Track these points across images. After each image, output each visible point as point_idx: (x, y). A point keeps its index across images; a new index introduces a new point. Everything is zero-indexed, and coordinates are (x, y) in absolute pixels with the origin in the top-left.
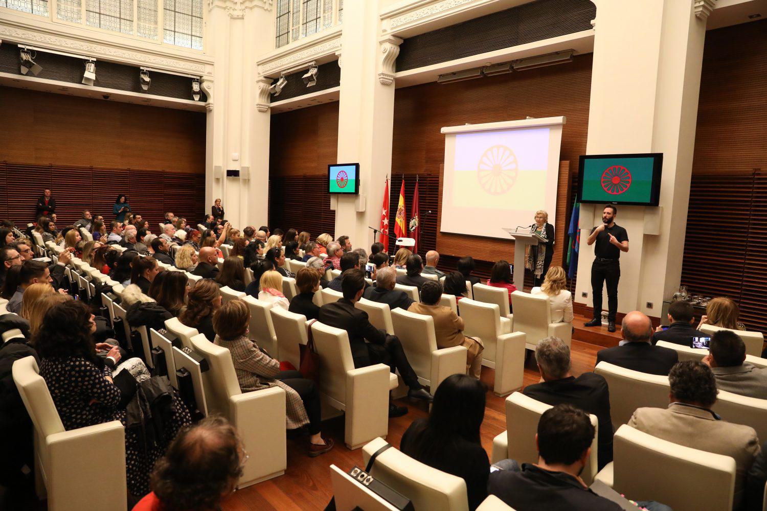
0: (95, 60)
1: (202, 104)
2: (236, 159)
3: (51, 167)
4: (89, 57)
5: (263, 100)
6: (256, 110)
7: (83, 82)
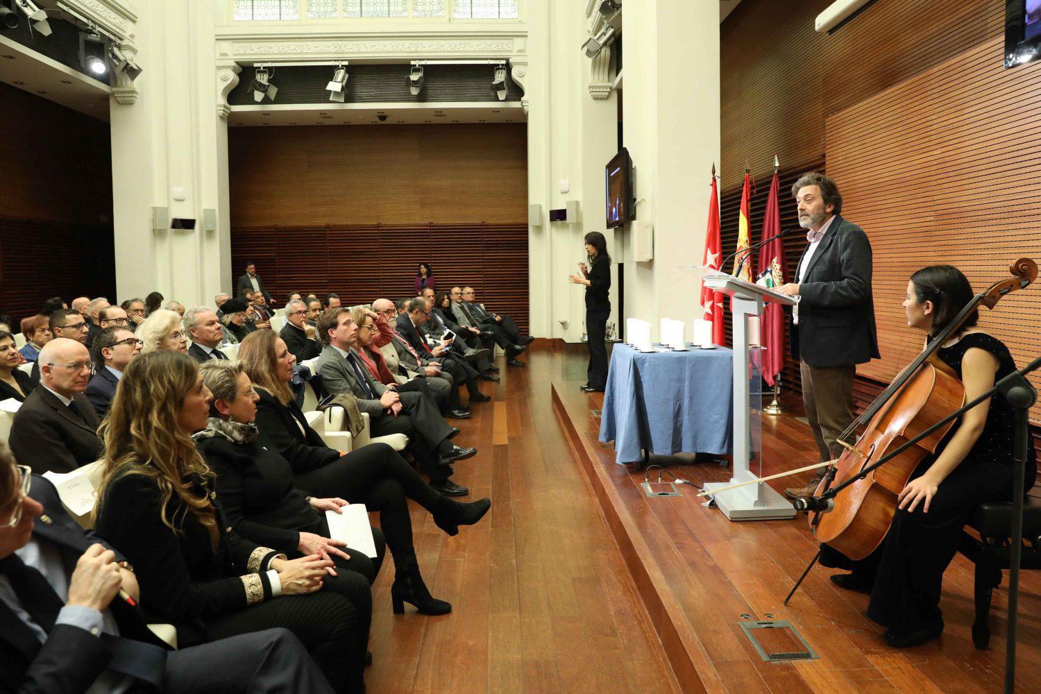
0: (346, 63)
1: (515, 105)
3: (328, 227)
4: (338, 61)
5: (601, 77)
7: (331, 99)
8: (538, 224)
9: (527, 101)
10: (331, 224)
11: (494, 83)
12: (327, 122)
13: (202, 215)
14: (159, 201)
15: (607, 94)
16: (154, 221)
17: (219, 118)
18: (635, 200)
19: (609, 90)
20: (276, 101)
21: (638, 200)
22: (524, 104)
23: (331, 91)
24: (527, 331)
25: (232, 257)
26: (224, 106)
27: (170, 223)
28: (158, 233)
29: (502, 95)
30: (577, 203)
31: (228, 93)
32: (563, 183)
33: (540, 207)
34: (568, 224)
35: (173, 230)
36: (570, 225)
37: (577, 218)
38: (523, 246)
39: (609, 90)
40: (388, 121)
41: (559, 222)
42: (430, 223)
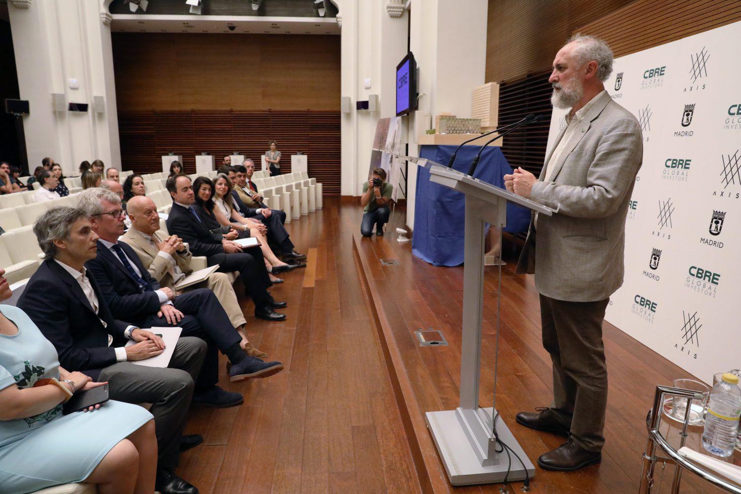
2: (369, 85)
3: (193, 111)
6: (387, 14)
7: (191, 11)
8: (348, 112)
9: (340, 18)
10: (195, 109)
11: (316, 2)
12: (190, 31)
13: (93, 101)
14: (57, 89)
15: (401, 13)
16: (54, 104)
17: (103, 25)
18: (418, 94)
19: (402, 10)
20: (148, 12)
21: (420, 94)
22: (338, 20)
23: (190, 6)
24: (339, 191)
25: (120, 133)
26: (106, 14)
27: (67, 106)
28: (58, 115)
29: (322, 12)
30: (377, 96)
31: (108, 5)
32: (367, 81)
33: (350, 99)
34: (370, 112)
35: (71, 112)
36: (372, 113)
37: (376, 108)
38: (338, 127)
39: (402, 10)
40: (235, 31)
41: (363, 111)
42: (270, 109)
